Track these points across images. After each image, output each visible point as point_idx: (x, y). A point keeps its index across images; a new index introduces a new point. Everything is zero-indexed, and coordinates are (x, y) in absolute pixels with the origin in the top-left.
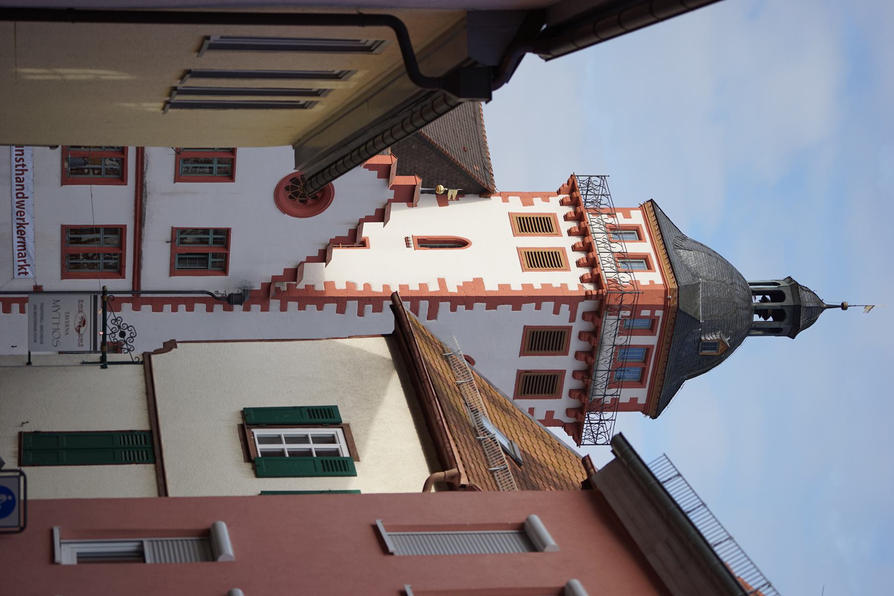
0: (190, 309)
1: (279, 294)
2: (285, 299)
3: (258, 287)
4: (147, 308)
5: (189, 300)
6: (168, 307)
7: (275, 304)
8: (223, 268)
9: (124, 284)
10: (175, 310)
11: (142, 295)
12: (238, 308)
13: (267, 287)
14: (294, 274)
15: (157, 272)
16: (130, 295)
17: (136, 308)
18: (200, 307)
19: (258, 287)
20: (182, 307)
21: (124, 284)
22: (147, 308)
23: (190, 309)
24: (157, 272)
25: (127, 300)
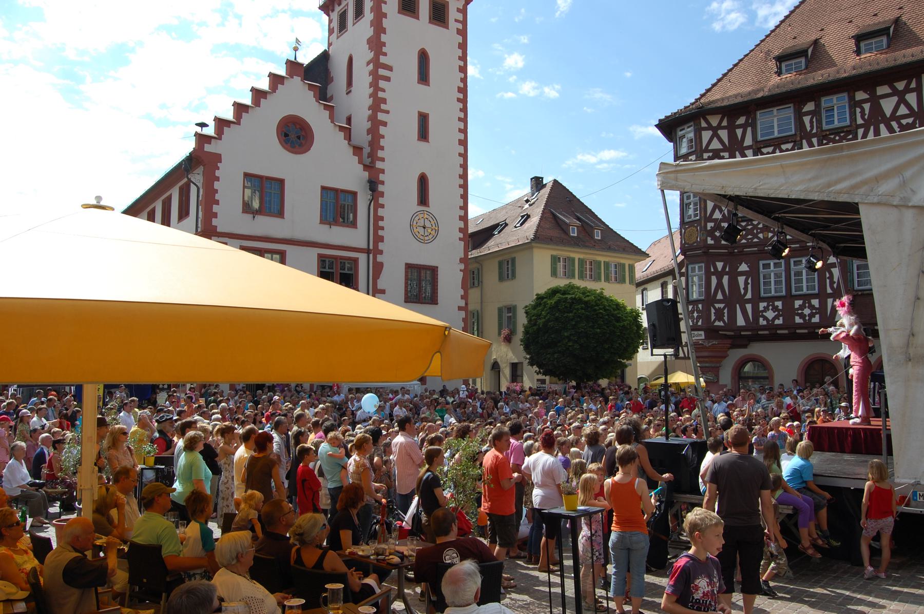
0: (382, 219)
1: (373, 162)
2: (373, 156)
3: (367, 174)
4: (381, 246)
5: (376, 222)
6: (380, 233)
7: (379, 165)
8: (354, 194)
9: (362, 258)
10: (382, 228)
11: (371, 247)
12: (381, 188)
13: (367, 167)
14: (357, 150)
15: (356, 237)
16: (371, 256)
17: (381, 252)
18: (381, 212)
19: (367, 174)
20: (381, 223)
21: (362, 258)
22: (381, 246)
23: (382, 219)
24: (356, 237)
25: (375, 258)
